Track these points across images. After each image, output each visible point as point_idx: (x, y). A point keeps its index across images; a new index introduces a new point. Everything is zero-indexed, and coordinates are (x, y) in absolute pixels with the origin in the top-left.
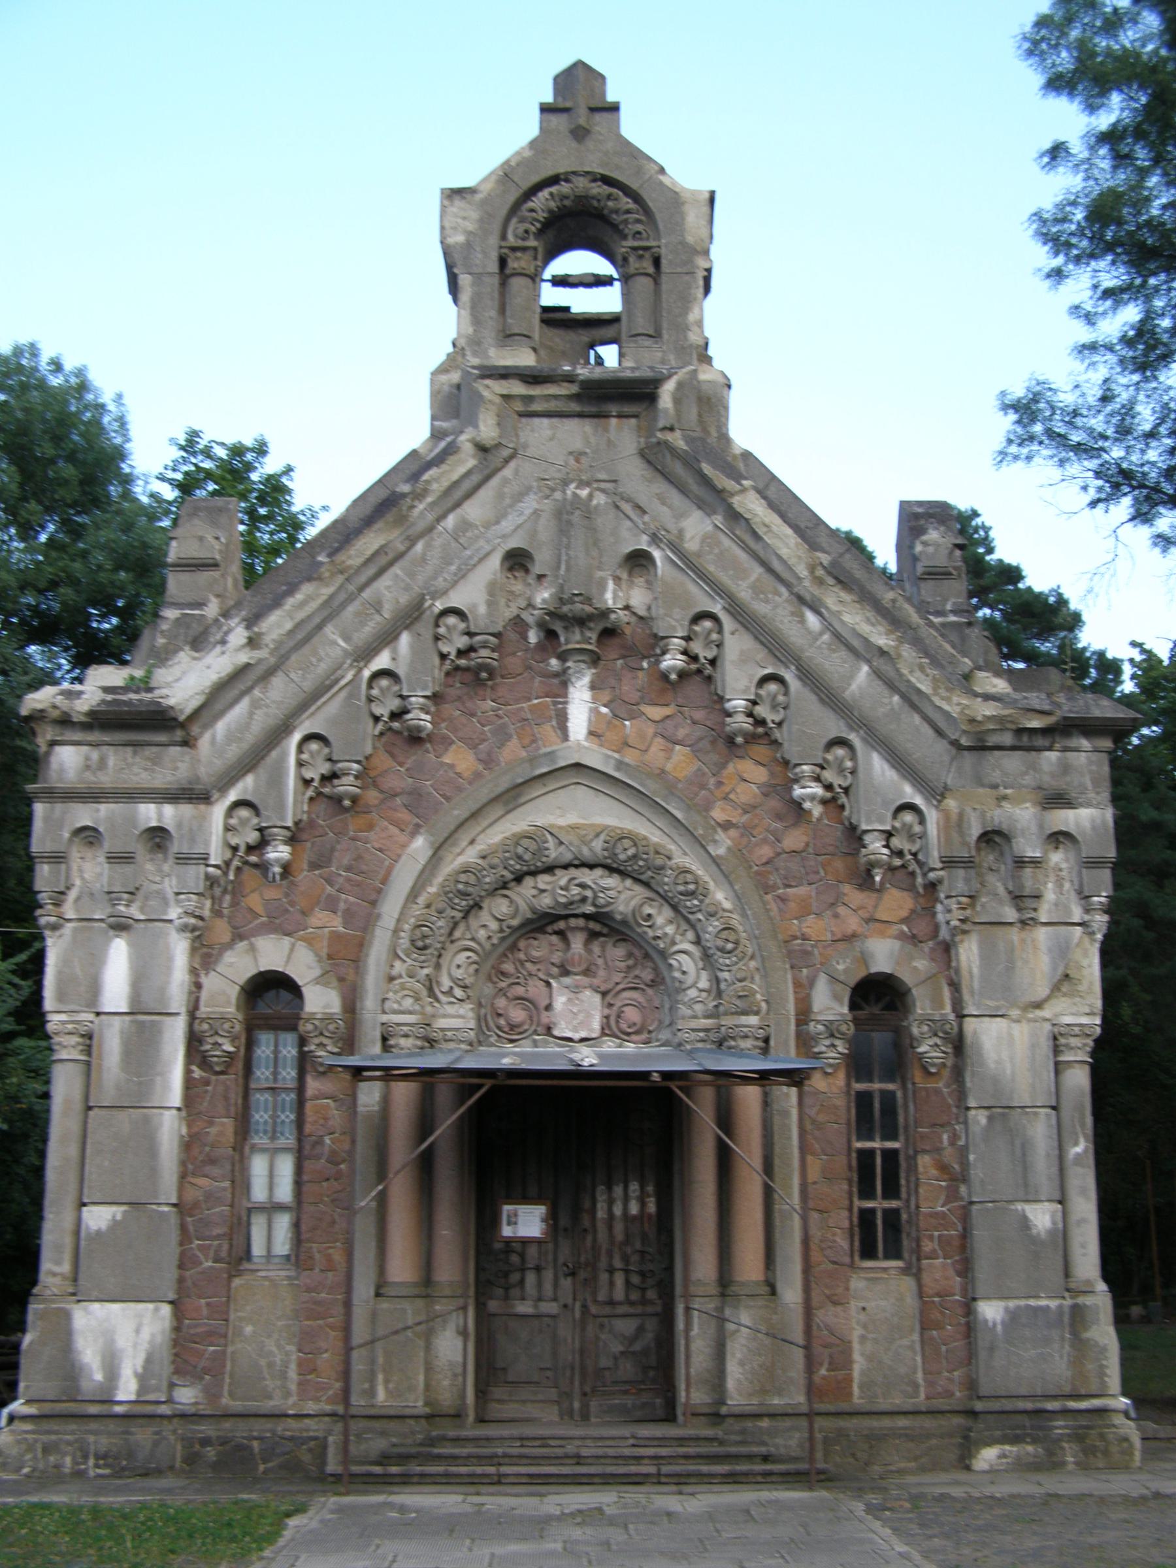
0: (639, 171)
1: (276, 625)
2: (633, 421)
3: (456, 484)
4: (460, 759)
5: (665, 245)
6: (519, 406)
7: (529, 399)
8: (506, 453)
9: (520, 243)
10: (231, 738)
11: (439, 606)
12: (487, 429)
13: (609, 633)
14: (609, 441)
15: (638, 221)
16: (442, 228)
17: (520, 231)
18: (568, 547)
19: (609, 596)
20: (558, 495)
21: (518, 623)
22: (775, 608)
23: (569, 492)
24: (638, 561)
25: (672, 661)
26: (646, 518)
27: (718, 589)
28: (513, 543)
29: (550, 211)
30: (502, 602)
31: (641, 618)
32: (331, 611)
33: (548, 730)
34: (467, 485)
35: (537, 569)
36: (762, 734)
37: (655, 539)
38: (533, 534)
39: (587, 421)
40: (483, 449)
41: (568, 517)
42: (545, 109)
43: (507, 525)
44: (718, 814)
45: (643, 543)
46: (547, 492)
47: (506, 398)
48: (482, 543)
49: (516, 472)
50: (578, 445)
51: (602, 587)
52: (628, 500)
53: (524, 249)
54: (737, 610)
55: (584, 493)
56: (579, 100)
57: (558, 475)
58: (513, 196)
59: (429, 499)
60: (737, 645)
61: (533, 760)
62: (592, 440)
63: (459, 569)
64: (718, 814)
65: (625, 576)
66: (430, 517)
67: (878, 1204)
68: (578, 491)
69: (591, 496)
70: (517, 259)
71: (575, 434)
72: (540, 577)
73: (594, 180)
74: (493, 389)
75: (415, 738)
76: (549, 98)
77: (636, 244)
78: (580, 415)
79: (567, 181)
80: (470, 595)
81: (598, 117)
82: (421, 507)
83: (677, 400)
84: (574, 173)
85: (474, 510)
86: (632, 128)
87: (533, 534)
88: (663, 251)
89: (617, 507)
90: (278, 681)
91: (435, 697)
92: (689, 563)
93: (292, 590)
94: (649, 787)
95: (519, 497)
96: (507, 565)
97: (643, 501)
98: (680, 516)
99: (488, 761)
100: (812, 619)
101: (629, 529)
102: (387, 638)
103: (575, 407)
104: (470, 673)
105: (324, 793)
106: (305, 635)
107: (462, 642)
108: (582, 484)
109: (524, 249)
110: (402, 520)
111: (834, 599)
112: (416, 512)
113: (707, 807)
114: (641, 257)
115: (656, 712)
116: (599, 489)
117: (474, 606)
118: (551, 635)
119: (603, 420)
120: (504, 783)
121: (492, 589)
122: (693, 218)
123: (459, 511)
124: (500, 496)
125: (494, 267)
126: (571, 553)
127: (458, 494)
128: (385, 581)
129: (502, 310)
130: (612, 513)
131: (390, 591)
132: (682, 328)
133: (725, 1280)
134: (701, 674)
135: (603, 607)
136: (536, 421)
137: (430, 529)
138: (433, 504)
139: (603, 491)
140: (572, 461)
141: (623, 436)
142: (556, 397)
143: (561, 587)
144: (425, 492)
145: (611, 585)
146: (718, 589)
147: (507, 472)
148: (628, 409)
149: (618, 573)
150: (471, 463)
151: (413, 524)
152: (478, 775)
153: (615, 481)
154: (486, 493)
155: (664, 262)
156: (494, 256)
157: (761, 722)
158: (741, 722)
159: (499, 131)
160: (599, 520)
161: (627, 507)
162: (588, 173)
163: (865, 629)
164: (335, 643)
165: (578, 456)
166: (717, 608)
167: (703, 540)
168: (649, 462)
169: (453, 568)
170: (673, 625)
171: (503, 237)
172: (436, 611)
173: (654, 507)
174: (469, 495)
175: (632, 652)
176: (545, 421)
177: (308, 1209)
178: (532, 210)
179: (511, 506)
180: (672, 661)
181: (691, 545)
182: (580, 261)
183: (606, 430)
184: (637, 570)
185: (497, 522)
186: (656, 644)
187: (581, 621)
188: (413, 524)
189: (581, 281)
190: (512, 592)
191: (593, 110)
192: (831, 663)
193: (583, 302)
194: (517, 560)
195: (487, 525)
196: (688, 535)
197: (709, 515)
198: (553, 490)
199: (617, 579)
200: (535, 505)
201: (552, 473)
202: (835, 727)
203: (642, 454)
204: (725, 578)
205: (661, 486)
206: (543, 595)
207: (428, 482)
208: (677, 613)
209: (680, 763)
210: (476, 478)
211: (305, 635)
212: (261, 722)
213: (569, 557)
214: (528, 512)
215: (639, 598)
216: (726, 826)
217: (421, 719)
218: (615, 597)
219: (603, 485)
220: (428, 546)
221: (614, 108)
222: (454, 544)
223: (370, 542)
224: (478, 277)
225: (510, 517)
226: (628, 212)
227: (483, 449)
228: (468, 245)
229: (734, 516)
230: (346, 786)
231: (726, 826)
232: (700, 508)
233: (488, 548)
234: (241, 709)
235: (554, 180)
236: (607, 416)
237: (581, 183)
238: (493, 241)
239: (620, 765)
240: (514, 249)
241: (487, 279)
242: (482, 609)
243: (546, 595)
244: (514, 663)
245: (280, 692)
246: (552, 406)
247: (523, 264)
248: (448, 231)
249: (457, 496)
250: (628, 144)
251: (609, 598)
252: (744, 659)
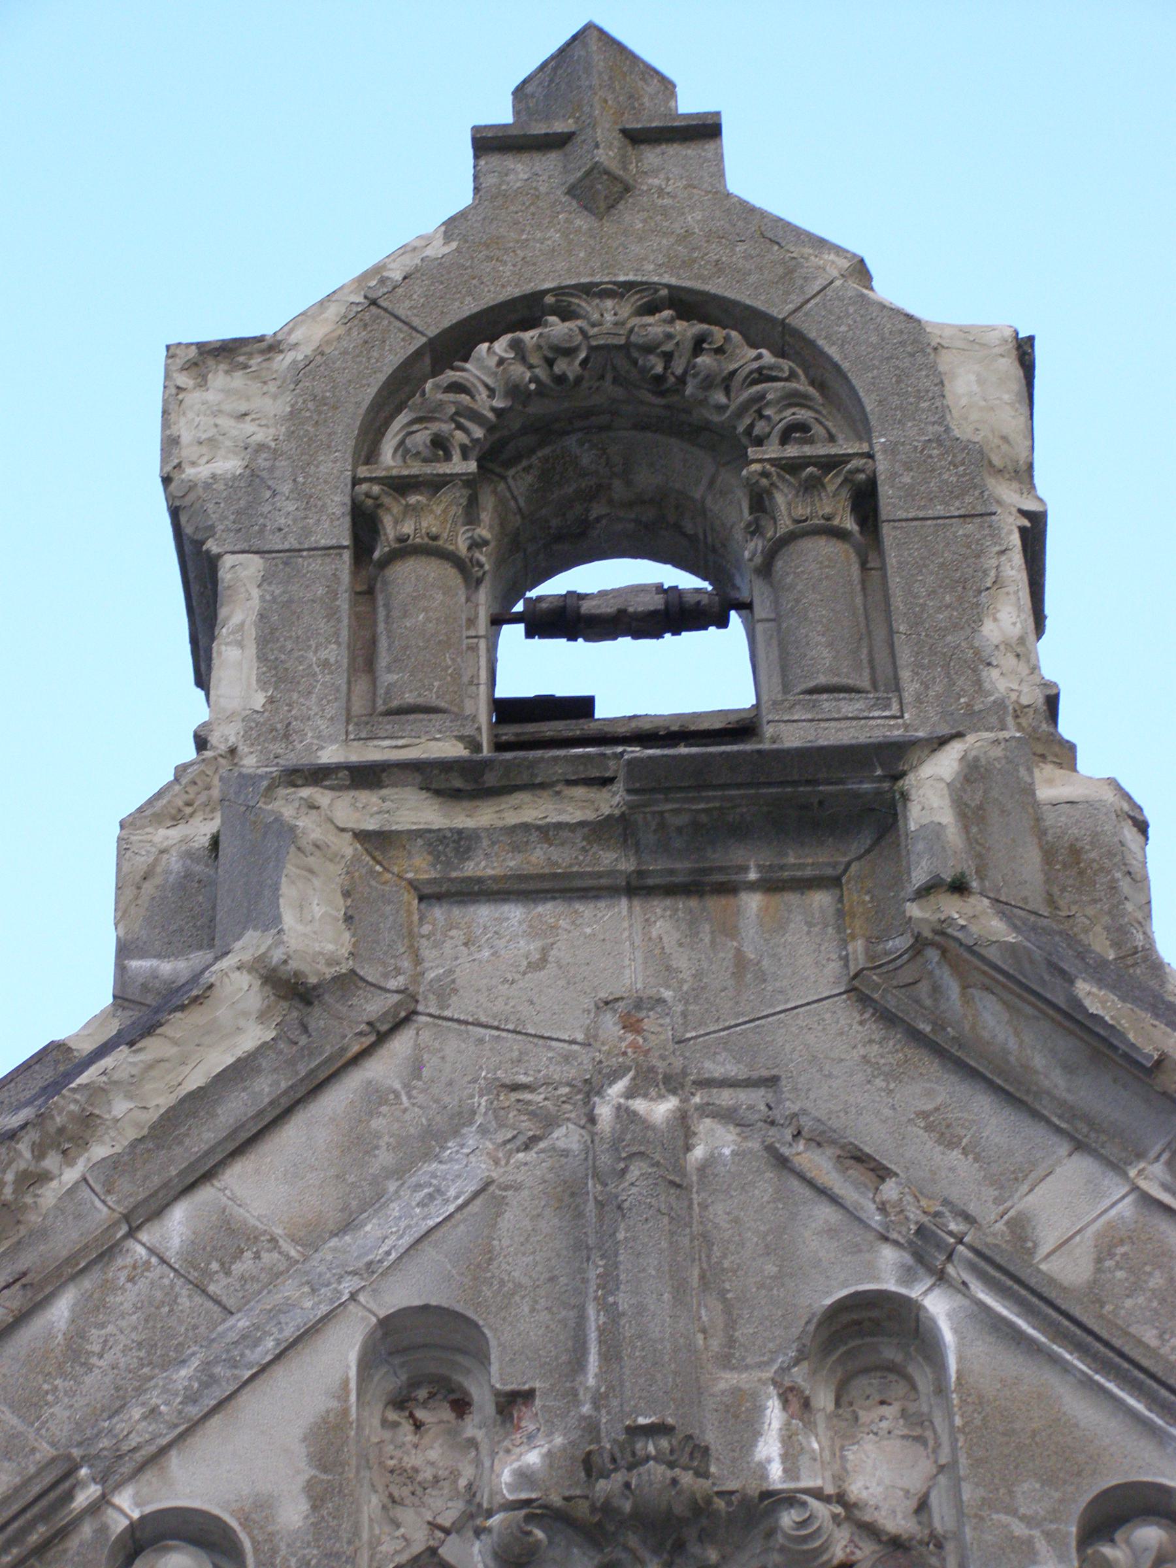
0: (790, 272)
2: (821, 900)
3: (196, 1103)
6: (421, 866)
7: (461, 843)
8: (375, 1006)
9: (416, 468)
11: (128, 1506)
12: (309, 925)
14: (741, 964)
15: (795, 399)
16: (170, 443)
17: (421, 438)
18: (609, 1282)
19: (769, 1449)
20: (567, 1137)
23: (604, 1112)
24: (867, 1341)
26: (890, 1190)
28: (400, 1295)
29: (514, 391)
30: (372, 1504)
31: (896, 1544)
34: (235, 1109)
35: (501, 1374)
37: (928, 1250)
38: (480, 1262)
39: (659, 906)
40: (292, 991)
41: (610, 1197)
42: (487, 143)
43: (384, 1234)
45: (887, 1272)
46: (529, 1127)
47: (377, 842)
48: (289, 1289)
49: (416, 1068)
50: (632, 977)
51: (747, 1425)
52: (817, 1142)
53: (435, 485)
55: (660, 1110)
56: (594, 123)
57: (571, 1072)
58: (396, 350)
59: (99, 1151)
62: (682, 962)
63: (208, 1379)
65: (824, 1400)
66: (102, 1211)
68: (639, 1105)
69: (683, 1122)
70: (410, 510)
71: (620, 945)
72: (511, 1403)
73: (650, 309)
76: (502, 114)
77: (792, 451)
78: (636, 888)
79: (566, 314)
81: (652, 156)
82: (71, 1175)
84: (588, 290)
85: (258, 1190)
86: (753, 172)
87: (480, 1262)
88: (882, 465)
89: (782, 1163)
95: (430, 1141)
96: (388, 1382)
97: (873, 1138)
98: (1009, 1179)
101: (831, 1232)
103: (612, 860)
108: (648, 1081)
109: (435, 485)
112: (50, 1194)
114: (812, 487)
116: (708, 1110)
117: (261, 1508)
119: (714, 904)
121: (328, 1444)
123: (206, 1194)
124: (358, 1143)
126: (624, 1301)
127: (205, 1136)
129: (365, 659)
130: (766, 1184)
135: (753, 1489)
136: (484, 913)
137: (107, 1253)
138: (113, 1166)
139: (728, 1116)
140: (610, 1026)
141: (789, 949)
142: (547, 832)
143: (591, 1428)
144: (87, 1125)
145: (774, 1415)
147: (385, 1067)
148: (802, 859)
149: (799, 1375)
150: (253, 1036)
151: (42, 1234)
153: (771, 1082)
155: (886, 493)
156: (337, 503)
159: (351, 188)
160: (719, 1211)
161: (819, 1164)
162: (629, 286)
165: (633, 1012)
167: (1105, 1249)
168: (888, 1018)
169: (183, 1374)
171: (368, 451)
172: (119, 1524)
173: (917, 1154)
174: (245, 1142)
176: (514, 913)
178: (457, 388)
179: (399, 1172)
181: (1068, 1269)
183: (729, 930)
184: (864, 1385)
185: (347, 1226)
188: (42, 1234)
190: (408, 1475)
191: (636, 138)
194: (425, 1364)
195: (311, 1237)
196: (1047, 1239)
197: (1117, 1167)
198: (550, 1122)
199: (797, 1402)
200: (482, 1168)
201: (542, 1064)
203: (858, 991)
205: (934, 1089)
206: (524, 1461)
207: (96, 1092)
208: (1030, 1495)
210: (266, 1087)
213: (613, 1314)
214: (458, 1190)
215: (881, 1473)
218: (791, 1456)
219: (725, 1098)
220: (92, 1310)
222: (186, 1300)
224: (283, 560)
225: (395, 1209)
226: (762, 376)
227: (292, 991)
232: (1080, 1146)
233: (311, 1308)
235: (523, 312)
236: (729, 889)
238: (334, 471)
240: (401, 486)
241: (315, 565)
242: (293, 1514)
243: (533, 1458)
246: (538, 858)
247: (430, 523)
248: (187, 451)
249: (199, 1146)
250: (749, 211)
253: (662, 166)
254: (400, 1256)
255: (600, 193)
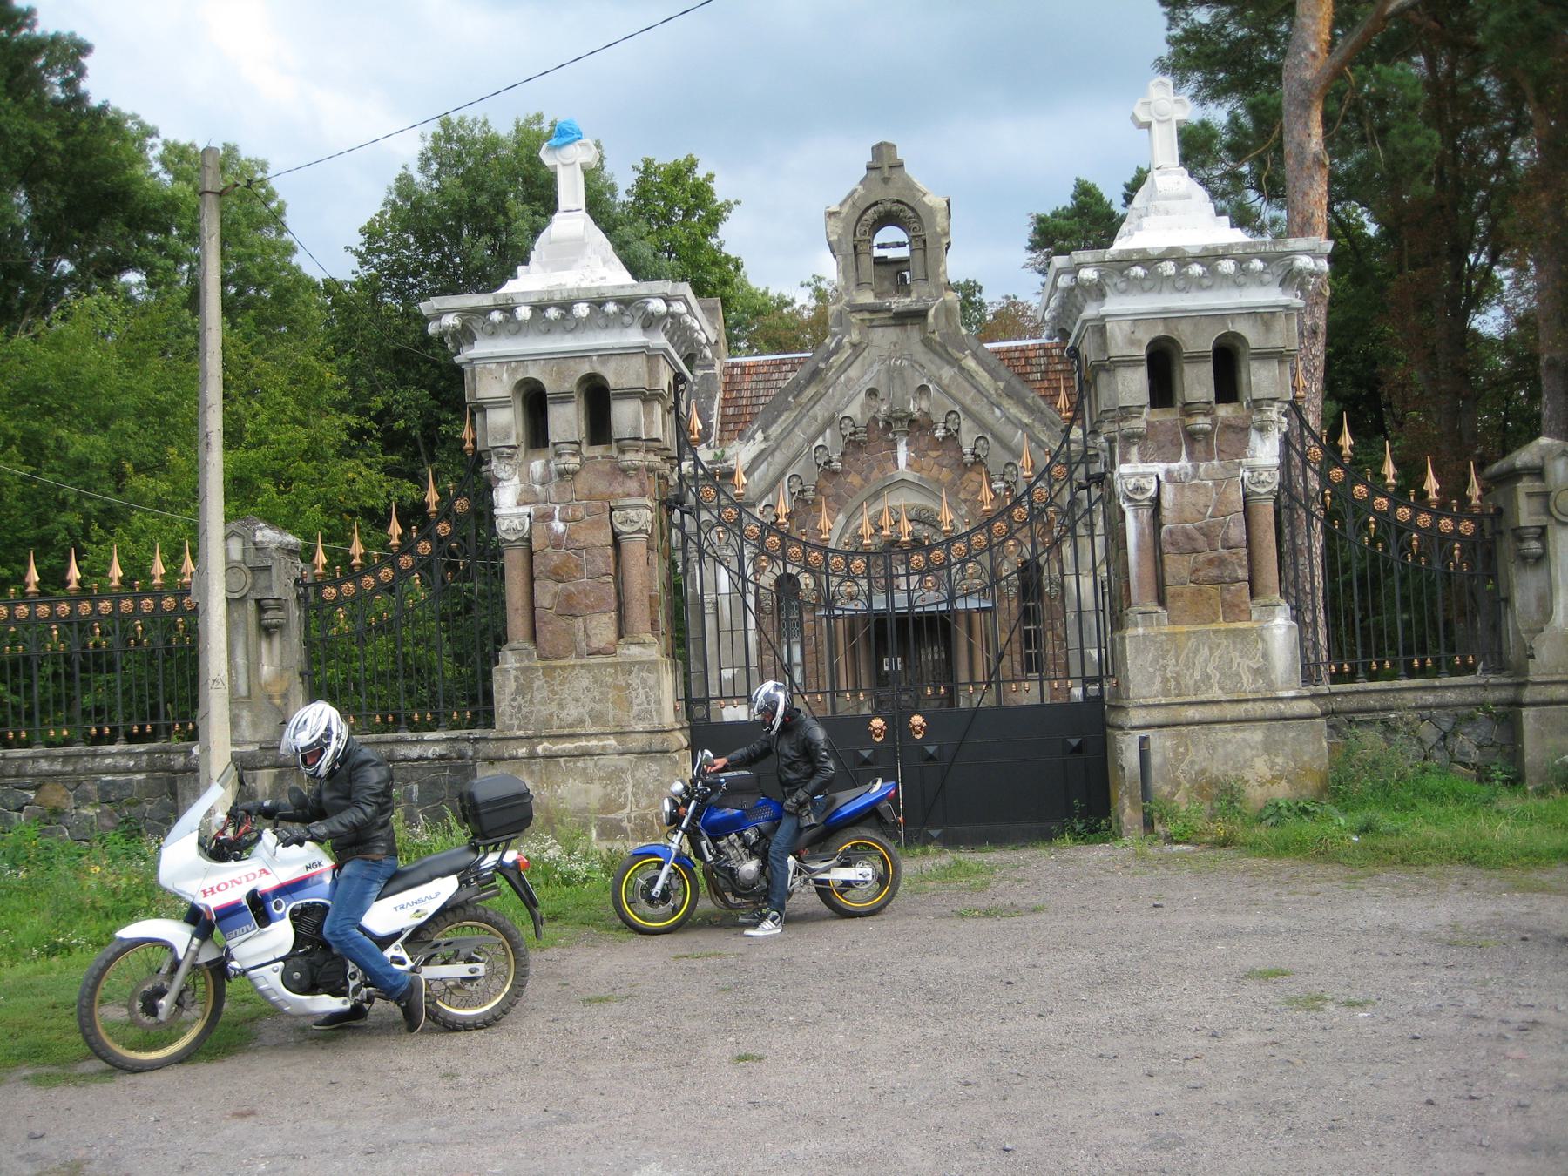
1: (775, 431)
4: (854, 479)
5: (927, 234)
7: (872, 320)
10: (761, 479)
12: (855, 336)
13: (912, 422)
21: (875, 419)
22: (982, 408)
24: (923, 389)
25: (940, 433)
27: (956, 401)
32: (796, 422)
33: (890, 464)
35: (881, 396)
36: (978, 461)
40: (854, 346)
41: (891, 372)
43: (867, 378)
44: (962, 496)
50: (894, 339)
54: (965, 409)
56: (884, 163)
60: (966, 425)
61: (884, 480)
64: (962, 496)
67: (1033, 651)
71: (892, 334)
74: (855, 318)
75: (835, 473)
80: (854, 410)
83: (935, 317)
90: (777, 454)
91: (843, 454)
92: (945, 390)
93: (779, 416)
94: (933, 487)
95: (871, 365)
98: (940, 369)
99: (866, 480)
100: (997, 411)
102: (821, 432)
104: (854, 445)
105: (800, 499)
106: (787, 433)
107: (852, 430)
110: (822, 380)
111: (1006, 403)
113: (957, 494)
115: (934, 454)
118: (888, 424)
120: (873, 490)
121: (862, 407)
122: (940, 219)
125: (851, 251)
128: (817, 407)
131: (820, 412)
132: (938, 275)
133: (972, 682)
134: (952, 437)
146: (956, 401)
152: (862, 487)
154: (857, 364)
157: (977, 456)
158: (969, 458)
163: (1019, 415)
164: (799, 436)
166: (957, 409)
170: (939, 418)
173: (928, 365)
175: (921, 428)
177: (808, 665)
180: (940, 433)
181: (945, 381)
182: (891, 234)
186: (932, 426)
187: (901, 419)
189: (891, 241)
192: (1006, 430)
193: (891, 254)
194: (872, 393)
202: (1008, 458)
204: (960, 396)
205: (931, 356)
206: (884, 408)
209: (945, 475)
211: (787, 433)
212: (773, 472)
215: (924, 405)
216: (965, 501)
217: (838, 465)
221: (901, 165)
223: (810, 391)
228: (839, 240)
229: (962, 369)
230: (810, 495)
231: (965, 501)
234: (763, 467)
237: (888, 205)
238: (850, 238)
239: (920, 479)
244: (874, 436)
245: (779, 458)
249: (844, 367)
251: (912, 407)
252: (969, 431)
253: (895, 173)
254: (868, 381)
255: (886, 180)
